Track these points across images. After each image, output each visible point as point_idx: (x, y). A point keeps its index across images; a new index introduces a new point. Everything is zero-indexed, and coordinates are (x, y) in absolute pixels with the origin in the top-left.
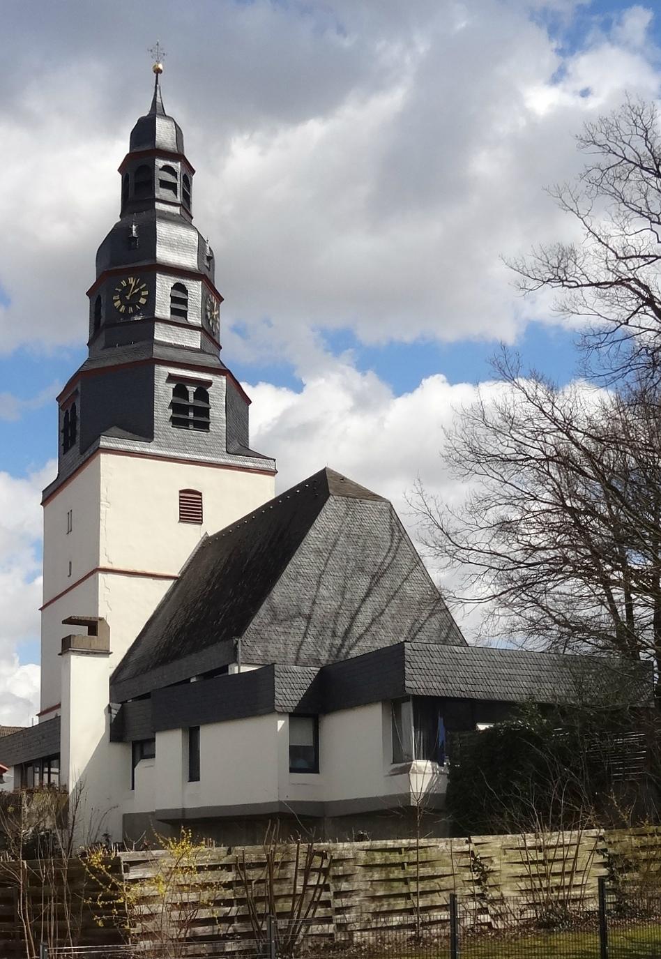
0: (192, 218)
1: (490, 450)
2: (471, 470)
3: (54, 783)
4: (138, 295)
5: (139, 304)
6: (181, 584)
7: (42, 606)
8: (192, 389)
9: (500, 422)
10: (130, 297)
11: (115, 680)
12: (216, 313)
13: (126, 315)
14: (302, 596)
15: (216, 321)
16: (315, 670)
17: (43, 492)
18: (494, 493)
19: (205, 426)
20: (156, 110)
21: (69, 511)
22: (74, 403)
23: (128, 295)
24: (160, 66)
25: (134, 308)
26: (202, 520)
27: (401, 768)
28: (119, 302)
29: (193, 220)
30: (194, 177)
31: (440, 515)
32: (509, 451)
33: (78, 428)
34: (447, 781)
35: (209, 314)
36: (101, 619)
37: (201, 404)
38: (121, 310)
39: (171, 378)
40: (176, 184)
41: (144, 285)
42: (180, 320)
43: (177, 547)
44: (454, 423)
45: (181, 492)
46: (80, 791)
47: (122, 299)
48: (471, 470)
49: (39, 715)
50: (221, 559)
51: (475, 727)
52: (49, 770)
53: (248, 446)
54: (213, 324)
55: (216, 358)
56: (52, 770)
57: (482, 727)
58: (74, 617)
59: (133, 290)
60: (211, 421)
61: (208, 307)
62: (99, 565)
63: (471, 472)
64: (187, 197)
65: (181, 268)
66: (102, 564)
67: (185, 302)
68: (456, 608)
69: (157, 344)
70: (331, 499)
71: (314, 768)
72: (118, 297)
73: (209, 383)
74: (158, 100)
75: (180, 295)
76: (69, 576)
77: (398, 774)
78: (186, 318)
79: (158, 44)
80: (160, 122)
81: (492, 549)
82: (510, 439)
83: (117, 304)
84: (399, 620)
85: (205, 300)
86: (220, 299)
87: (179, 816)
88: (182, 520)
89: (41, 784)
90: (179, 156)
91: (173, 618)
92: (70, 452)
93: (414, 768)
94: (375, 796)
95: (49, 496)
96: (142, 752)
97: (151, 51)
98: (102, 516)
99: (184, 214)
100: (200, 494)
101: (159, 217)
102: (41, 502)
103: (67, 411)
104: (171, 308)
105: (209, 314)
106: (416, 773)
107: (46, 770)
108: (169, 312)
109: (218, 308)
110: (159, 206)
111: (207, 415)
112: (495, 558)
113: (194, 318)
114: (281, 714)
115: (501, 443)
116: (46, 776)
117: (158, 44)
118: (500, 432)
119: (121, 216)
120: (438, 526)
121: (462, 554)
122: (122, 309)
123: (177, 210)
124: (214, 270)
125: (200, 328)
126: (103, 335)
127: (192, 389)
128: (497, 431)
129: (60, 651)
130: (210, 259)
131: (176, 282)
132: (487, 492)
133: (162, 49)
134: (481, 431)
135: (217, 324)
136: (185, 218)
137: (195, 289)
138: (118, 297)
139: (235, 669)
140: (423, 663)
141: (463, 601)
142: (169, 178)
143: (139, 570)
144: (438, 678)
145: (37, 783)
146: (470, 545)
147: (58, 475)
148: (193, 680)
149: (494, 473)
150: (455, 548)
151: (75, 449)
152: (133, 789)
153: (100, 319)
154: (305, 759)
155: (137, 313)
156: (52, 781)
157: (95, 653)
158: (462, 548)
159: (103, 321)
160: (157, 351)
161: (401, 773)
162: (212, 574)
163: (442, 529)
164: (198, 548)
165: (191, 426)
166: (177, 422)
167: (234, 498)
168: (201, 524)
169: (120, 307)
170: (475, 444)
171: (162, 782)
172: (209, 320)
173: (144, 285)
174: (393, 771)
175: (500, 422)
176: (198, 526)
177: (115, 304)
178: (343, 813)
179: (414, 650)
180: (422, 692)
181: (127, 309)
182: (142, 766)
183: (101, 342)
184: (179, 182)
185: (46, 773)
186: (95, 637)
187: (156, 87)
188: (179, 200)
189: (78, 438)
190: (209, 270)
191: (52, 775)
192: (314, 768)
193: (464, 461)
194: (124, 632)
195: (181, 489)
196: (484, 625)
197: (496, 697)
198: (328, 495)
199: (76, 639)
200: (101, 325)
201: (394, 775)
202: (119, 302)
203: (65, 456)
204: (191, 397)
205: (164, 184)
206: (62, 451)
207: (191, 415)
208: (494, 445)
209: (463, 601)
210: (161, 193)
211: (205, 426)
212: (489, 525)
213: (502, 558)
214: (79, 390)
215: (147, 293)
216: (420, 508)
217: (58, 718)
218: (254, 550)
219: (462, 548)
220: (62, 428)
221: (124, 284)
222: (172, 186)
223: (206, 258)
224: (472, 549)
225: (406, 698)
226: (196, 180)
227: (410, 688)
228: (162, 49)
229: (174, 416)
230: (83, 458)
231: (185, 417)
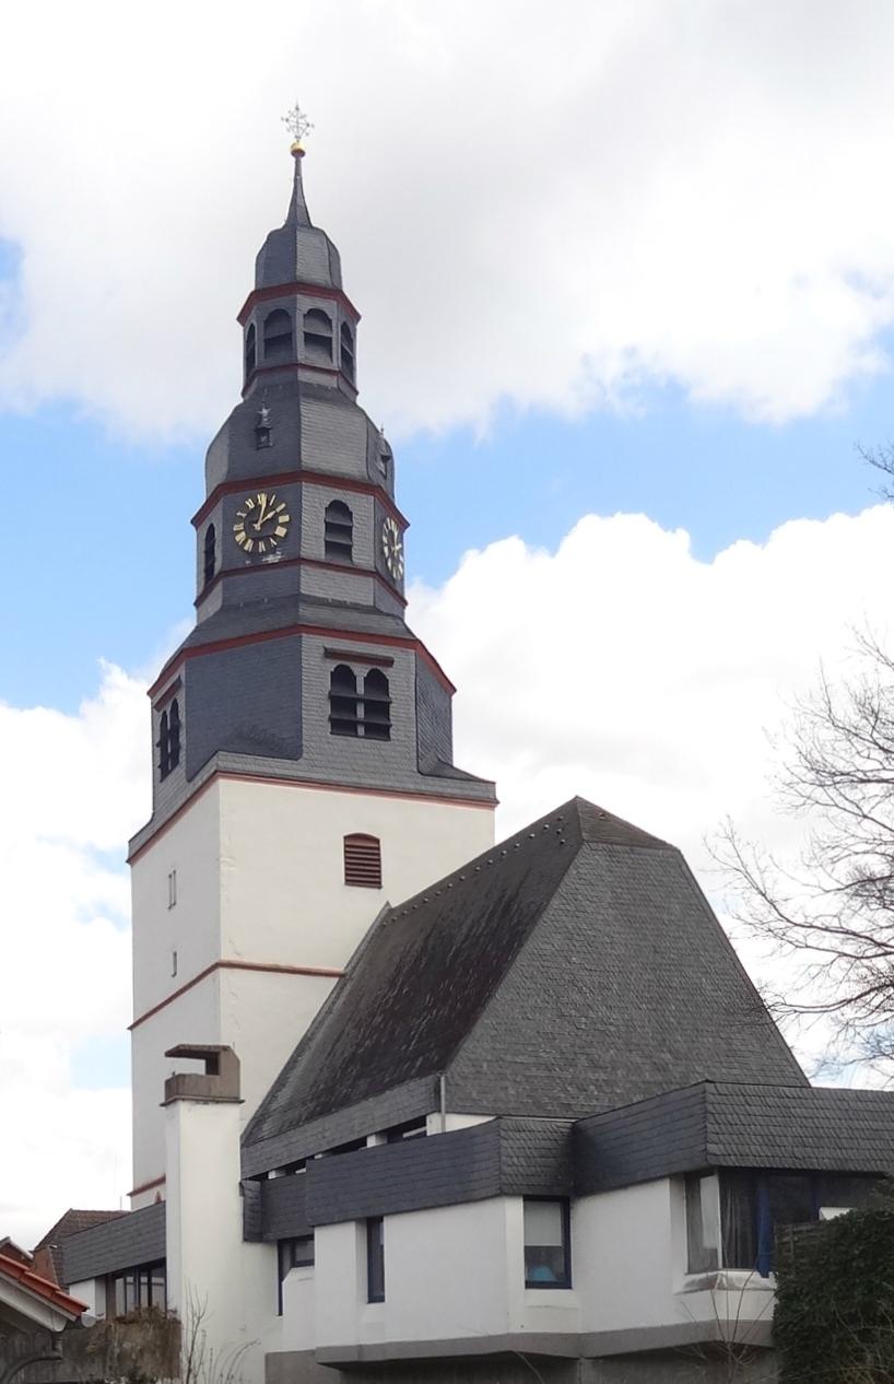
0: (357, 393)
1: (841, 766)
2: (809, 798)
3: (157, 1308)
4: (273, 522)
5: (275, 537)
6: (348, 987)
7: (132, 1023)
8: (361, 672)
9: (856, 719)
10: (261, 525)
11: (250, 1139)
12: (398, 547)
13: (254, 554)
14: (541, 1005)
15: (399, 560)
16: (563, 1124)
17: (130, 842)
18: (846, 835)
19: (380, 730)
20: (298, 214)
21: (171, 872)
22: (175, 701)
23: (256, 522)
24: (301, 146)
25: (267, 543)
26: (380, 883)
27: (701, 1281)
28: (243, 534)
29: (358, 398)
30: (359, 326)
31: (762, 872)
32: (869, 765)
33: (183, 739)
34: (775, 1301)
35: (386, 549)
36: (226, 1049)
37: (375, 698)
38: (246, 548)
39: (329, 654)
40: (330, 339)
41: (283, 505)
43: (342, 923)
44: (782, 722)
45: (345, 838)
46: (199, 1319)
47: (248, 529)
48: (809, 798)
49: (131, 1195)
50: (412, 946)
51: (817, 1214)
52: (149, 1280)
53: (451, 760)
54: (392, 566)
55: (399, 622)
56: (154, 1280)
57: (829, 1214)
58: (183, 1046)
59: (265, 515)
60: (392, 722)
61: (385, 539)
62: (218, 954)
63: (809, 801)
64: (348, 359)
65: (340, 476)
66: (225, 957)
67: (348, 531)
68: (787, 1021)
69: (305, 602)
70: (585, 848)
71: (564, 1282)
72: (241, 526)
73: (389, 662)
74: (299, 200)
77: (696, 1291)
78: (351, 559)
79: (297, 109)
80: (302, 237)
81: (844, 925)
82: (873, 746)
83: (240, 537)
84: (694, 1039)
85: (379, 526)
86: (403, 524)
87: (354, 1358)
88: (348, 882)
89: (138, 1308)
90: (336, 293)
91: (337, 1041)
92: (170, 778)
93: (721, 1281)
94: (660, 1325)
96: (293, 1253)
97: (287, 120)
98: (223, 880)
99: (344, 387)
100: (377, 841)
101: (305, 395)
102: (126, 858)
103: (165, 712)
104: (326, 542)
105: (386, 549)
106: (725, 1289)
107: (144, 1279)
108: (323, 549)
109: (401, 540)
110: (304, 376)
112: (848, 939)
113: (362, 555)
114: (512, 1194)
115: (858, 753)
116: (144, 1290)
117: (297, 109)
118: (857, 735)
119: (243, 394)
120: (757, 889)
121: (797, 934)
122: (249, 546)
123: (331, 382)
124: (392, 475)
125: (372, 572)
126: (219, 588)
127: (361, 672)
128: (852, 733)
129: (163, 1100)
130: (387, 459)
131: (331, 500)
132: (835, 833)
133: (302, 117)
134: (827, 734)
135: (400, 567)
136: (344, 393)
137: (362, 507)
138: (241, 526)
139: (433, 1126)
140: (735, 1116)
141: (799, 1011)
142: (319, 329)
143: (283, 963)
144: (759, 1138)
145: (131, 1308)
146: (810, 920)
147: (153, 815)
148: (372, 1142)
149: (847, 803)
150: (783, 924)
151: (179, 772)
152: (281, 1313)
153: (214, 562)
154: (550, 1267)
155: (272, 550)
156: (154, 1304)
157: (218, 1102)
158: (796, 925)
159: (218, 566)
160: (307, 613)
161: (702, 1290)
162: (399, 969)
163: (764, 895)
164: (375, 927)
165: (361, 730)
166: (342, 726)
167: (427, 847)
168: (380, 888)
169: (245, 542)
170: (817, 756)
171: (328, 1304)
173: (283, 505)
175: (856, 719)
176: (374, 891)
177: (238, 538)
178: (610, 1351)
179: (720, 1094)
180: (732, 1161)
181: (256, 546)
182: (294, 1276)
183: (215, 602)
184: (336, 335)
185: (144, 1284)
186: (217, 1077)
187: (296, 180)
188: (336, 364)
189: (182, 754)
190: (385, 477)
191: (153, 1287)
192: (564, 1282)
193: (798, 783)
194: (257, 1077)
195: (346, 834)
196: (831, 1047)
197: (851, 1167)
198: (581, 842)
199: (187, 1080)
200: (216, 572)
201: (691, 1292)
202: (243, 534)
203: (163, 783)
204: (361, 689)
205: (311, 339)
206: (159, 776)
207: (361, 711)
208: (847, 757)
209: (799, 1011)
210: (303, 353)
211: (380, 730)
212: (840, 886)
213: (860, 939)
214: (183, 679)
215: (284, 519)
216: (729, 861)
217: (160, 1204)
218: (465, 930)
219: (796, 925)
220: (157, 740)
221: (252, 506)
222: (323, 343)
223: (379, 458)
224: (811, 927)
225: (707, 1172)
226: (361, 330)
228: (302, 117)
230: (193, 787)
231: (353, 718)
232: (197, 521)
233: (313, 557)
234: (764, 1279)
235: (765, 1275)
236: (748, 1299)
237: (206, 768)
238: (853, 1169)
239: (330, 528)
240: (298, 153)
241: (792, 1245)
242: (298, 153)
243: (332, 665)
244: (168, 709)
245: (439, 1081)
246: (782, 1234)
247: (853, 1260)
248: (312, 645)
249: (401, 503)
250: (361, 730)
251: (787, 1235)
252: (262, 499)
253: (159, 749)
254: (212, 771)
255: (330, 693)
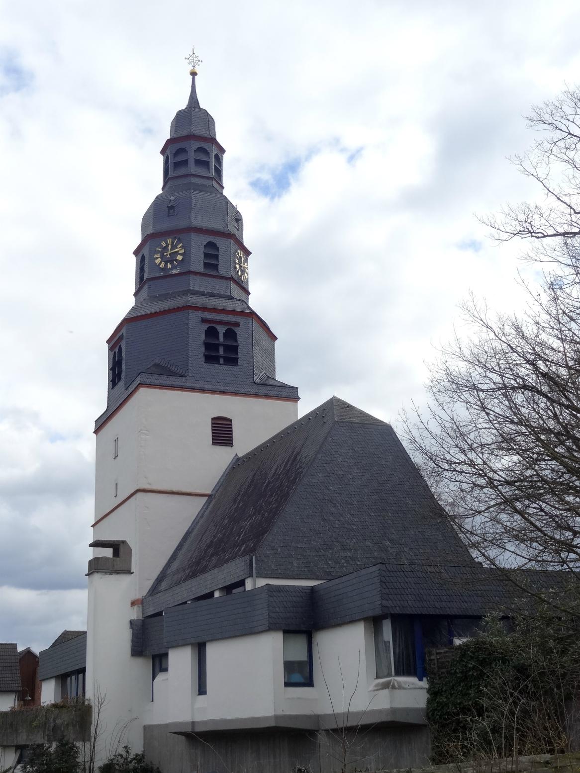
61: (237, 261)
67: (216, 257)
71: (309, 682)
76: (116, 496)
92: (117, 387)
95: (101, 424)
105: (238, 266)
172: (238, 272)
174: (376, 685)
190: (238, 230)
192: (309, 682)
200: (145, 279)
227: (387, 607)
229: (207, 354)
232: (136, 253)
233: (197, 271)
234: (421, 682)
235: (421, 680)
236: (411, 694)
237: (135, 382)
238: (471, 614)
239: (206, 255)
241: (436, 660)
243: (205, 327)
244: (117, 350)
245: (252, 558)
246: (430, 654)
247: (470, 670)
248: (195, 317)
249: (246, 243)
251: (434, 654)
253: (112, 371)
254: (137, 384)
255: (204, 342)
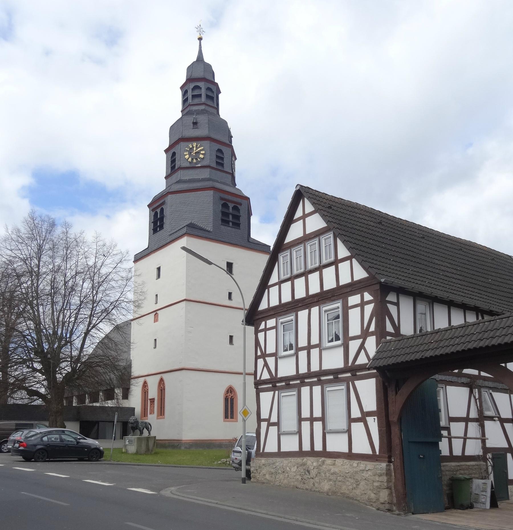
4: (198, 153)
8: (231, 205)
20: (200, 58)
37: (236, 213)
42: (220, 168)
47: (190, 154)
67: (222, 159)
72: (187, 153)
75: (220, 155)
83: (187, 157)
111: (239, 220)
138: (187, 153)
165: (231, 224)
169: (188, 158)
181: (192, 159)
204: (231, 210)
221: (191, 147)
240: (200, 39)
242: (200, 39)
250: (231, 224)
252: (195, 145)
